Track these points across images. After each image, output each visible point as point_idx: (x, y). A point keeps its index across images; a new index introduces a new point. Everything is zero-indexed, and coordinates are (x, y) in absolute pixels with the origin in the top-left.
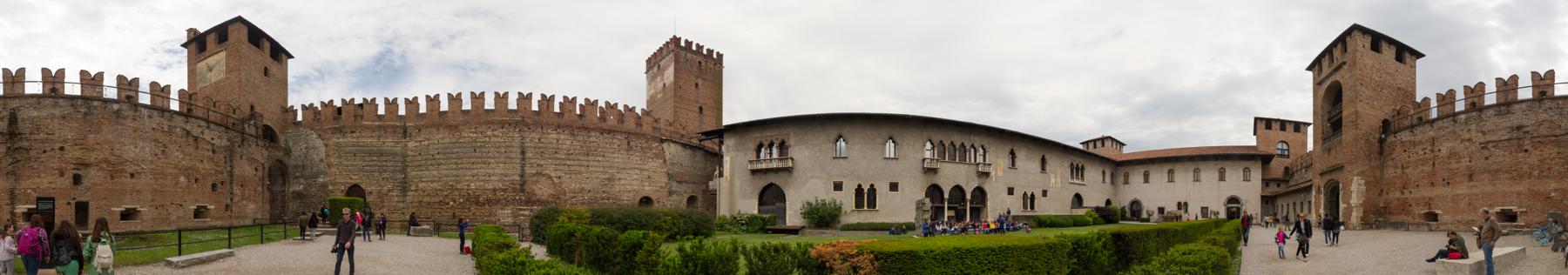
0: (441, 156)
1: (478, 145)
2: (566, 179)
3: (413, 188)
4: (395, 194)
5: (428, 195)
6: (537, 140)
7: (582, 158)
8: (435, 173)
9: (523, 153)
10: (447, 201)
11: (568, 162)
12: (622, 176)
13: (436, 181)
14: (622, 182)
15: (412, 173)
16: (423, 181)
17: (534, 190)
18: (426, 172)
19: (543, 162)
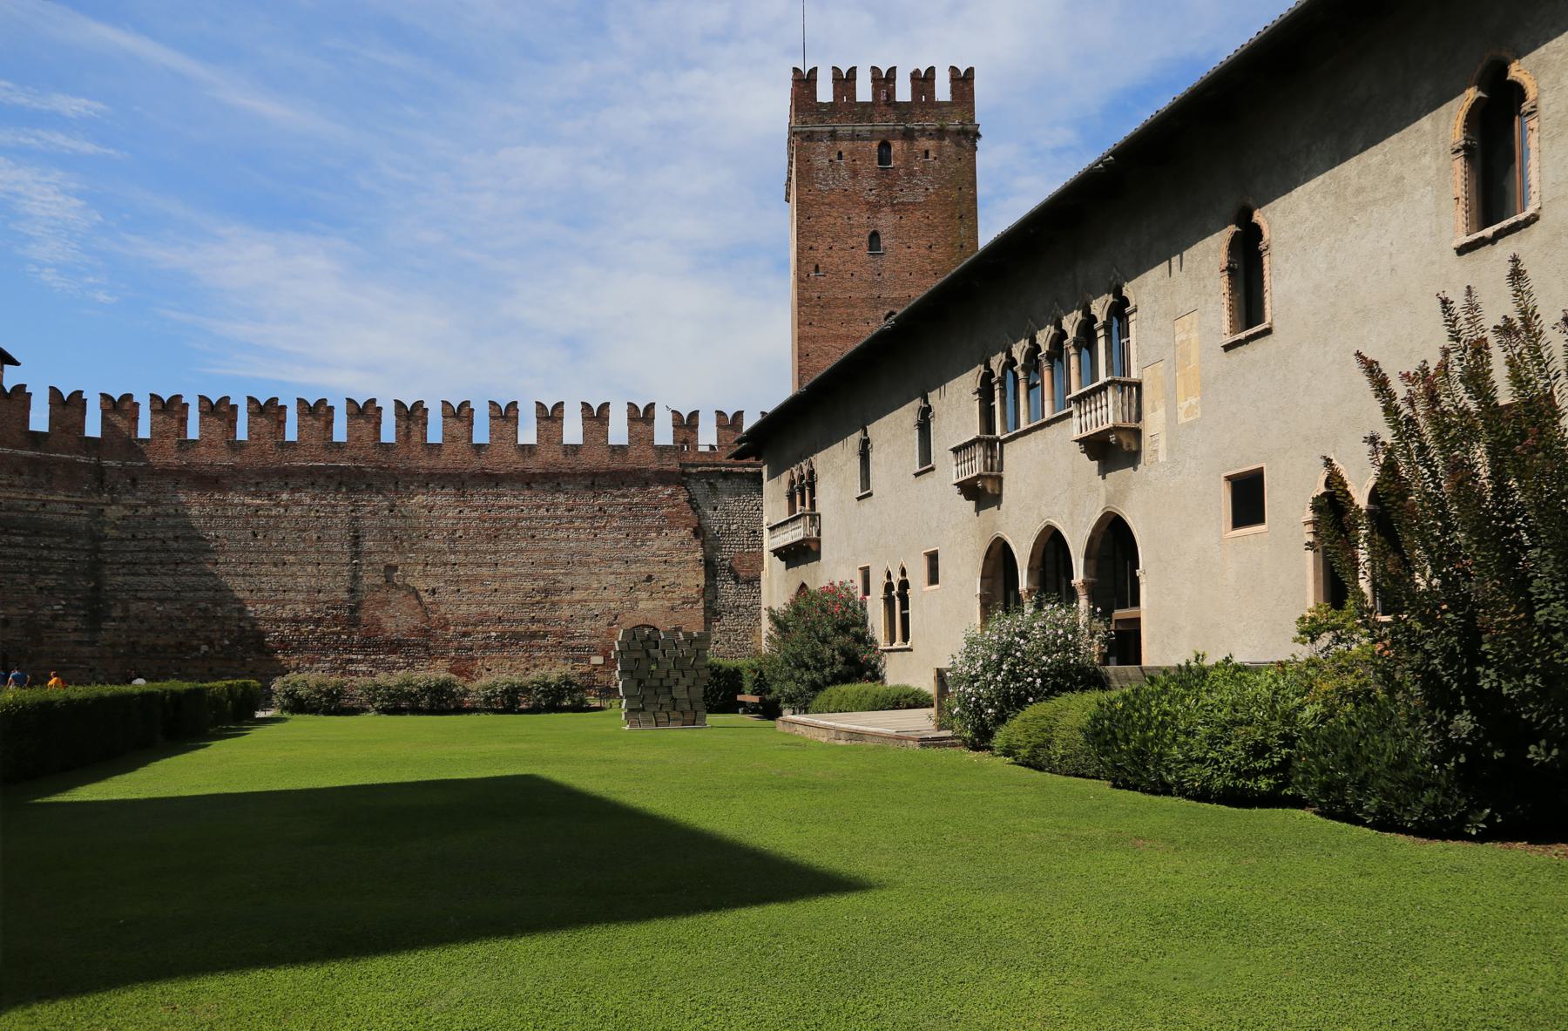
0: (184, 545)
1: (263, 522)
2: (446, 596)
3: (117, 612)
4: (72, 625)
5: (152, 629)
6: (386, 512)
7: (484, 547)
8: (168, 581)
9: (356, 540)
10: (195, 642)
11: (453, 557)
12: (579, 581)
13: (171, 599)
14: (577, 595)
15: (116, 580)
16: (141, 599)
17: (379, 620)
18: (148, 579)
19: (396, 560)
